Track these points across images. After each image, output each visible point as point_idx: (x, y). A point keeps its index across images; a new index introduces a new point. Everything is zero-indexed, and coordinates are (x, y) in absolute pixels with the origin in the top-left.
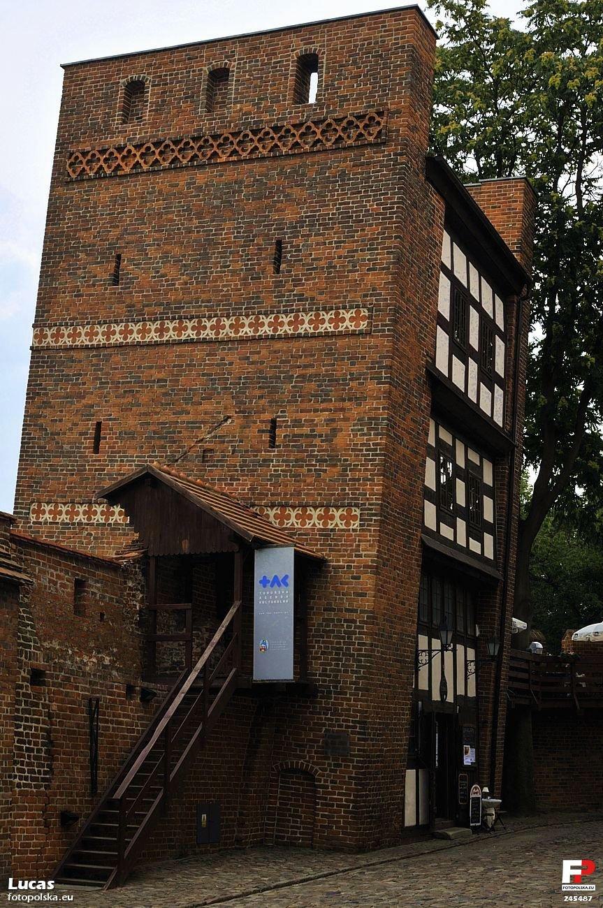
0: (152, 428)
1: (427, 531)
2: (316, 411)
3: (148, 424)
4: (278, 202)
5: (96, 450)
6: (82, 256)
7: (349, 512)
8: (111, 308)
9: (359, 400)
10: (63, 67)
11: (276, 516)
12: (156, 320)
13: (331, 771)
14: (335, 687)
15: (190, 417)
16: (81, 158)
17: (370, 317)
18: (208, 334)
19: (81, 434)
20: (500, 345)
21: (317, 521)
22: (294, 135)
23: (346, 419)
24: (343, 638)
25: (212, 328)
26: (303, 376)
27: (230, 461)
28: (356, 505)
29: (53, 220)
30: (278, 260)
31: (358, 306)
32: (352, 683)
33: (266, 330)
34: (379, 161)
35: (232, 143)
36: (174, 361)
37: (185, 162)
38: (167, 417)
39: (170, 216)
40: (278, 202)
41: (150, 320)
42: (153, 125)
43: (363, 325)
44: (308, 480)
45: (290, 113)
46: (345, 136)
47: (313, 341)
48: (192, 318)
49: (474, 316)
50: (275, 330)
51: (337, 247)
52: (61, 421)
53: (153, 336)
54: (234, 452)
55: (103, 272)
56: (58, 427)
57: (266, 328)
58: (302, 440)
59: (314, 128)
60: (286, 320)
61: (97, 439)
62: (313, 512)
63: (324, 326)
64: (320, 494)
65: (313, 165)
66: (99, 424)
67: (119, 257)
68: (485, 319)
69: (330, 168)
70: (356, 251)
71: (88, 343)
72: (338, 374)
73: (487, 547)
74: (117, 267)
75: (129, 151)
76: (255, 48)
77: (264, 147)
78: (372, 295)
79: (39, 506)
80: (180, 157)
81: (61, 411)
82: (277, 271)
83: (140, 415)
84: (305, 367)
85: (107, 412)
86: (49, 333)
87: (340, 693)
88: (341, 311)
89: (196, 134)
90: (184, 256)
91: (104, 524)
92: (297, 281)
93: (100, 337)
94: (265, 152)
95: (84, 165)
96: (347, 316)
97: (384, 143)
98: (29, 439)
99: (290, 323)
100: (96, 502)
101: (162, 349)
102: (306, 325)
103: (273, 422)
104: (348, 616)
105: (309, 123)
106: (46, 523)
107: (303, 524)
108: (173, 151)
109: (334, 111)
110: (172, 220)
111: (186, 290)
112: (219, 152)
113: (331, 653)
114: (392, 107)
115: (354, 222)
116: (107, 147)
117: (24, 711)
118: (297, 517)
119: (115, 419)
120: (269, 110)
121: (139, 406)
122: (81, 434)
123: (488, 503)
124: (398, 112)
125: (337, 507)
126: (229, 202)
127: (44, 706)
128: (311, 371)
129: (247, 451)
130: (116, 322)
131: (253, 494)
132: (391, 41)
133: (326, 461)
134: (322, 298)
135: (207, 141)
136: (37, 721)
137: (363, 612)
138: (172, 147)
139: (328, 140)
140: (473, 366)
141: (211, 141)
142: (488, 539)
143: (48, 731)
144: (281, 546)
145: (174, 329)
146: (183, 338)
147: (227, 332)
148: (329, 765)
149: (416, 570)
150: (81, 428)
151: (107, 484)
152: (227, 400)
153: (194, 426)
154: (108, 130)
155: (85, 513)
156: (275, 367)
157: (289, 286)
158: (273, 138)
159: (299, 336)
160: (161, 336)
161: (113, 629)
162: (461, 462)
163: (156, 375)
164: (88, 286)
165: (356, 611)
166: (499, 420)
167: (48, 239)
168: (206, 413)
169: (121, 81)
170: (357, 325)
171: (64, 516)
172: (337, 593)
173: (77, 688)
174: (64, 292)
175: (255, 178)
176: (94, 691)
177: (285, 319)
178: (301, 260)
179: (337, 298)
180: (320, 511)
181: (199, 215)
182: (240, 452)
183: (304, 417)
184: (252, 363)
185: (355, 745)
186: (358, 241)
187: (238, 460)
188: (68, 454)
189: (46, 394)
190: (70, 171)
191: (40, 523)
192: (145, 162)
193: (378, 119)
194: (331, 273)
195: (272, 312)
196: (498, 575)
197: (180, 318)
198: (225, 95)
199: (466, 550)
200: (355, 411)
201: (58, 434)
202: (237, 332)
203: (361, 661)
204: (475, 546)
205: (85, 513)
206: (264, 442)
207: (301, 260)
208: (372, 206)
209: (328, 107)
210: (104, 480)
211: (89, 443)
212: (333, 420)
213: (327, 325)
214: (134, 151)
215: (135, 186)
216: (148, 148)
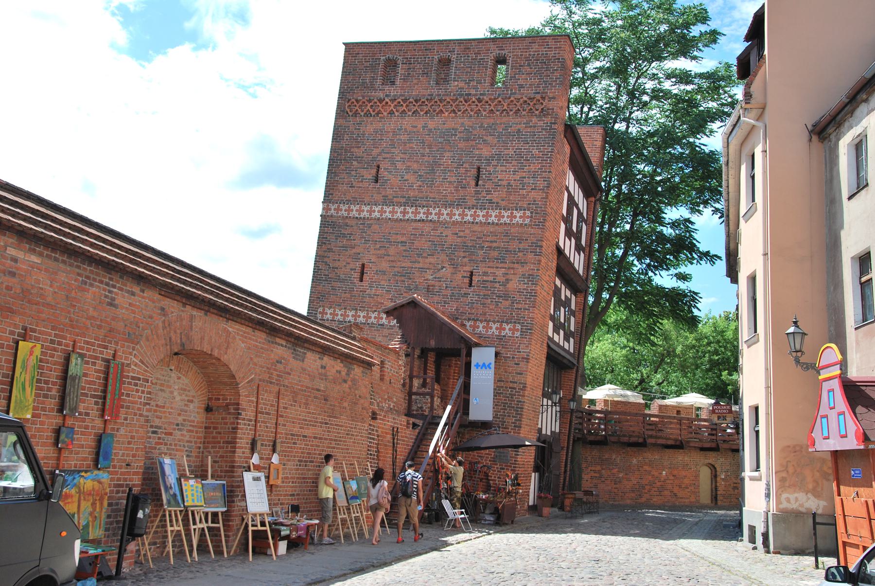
0: (396, 269)
1: (549, 338)
2: (497, 268)
3: (395, 267)
4: (479, 144)
5: (361, 280)
6: (355, 163)
7: (514, 326)
8: (372, 196)
9: (523, 263)
10: (344, 44)
11: (470, 326)
12: (401, 206)
13: (498, 471)
14: (503, 425)
15: (421, 265)
16: (355, 103)
17: (531, 217)
18: (433, 217)
19: (351, 270)
20: (584, 227)
21: (495, 331)
22: (490, 105)
23: (514, 274)
24: (508, 397)
25: (436, 214)
26: (490, 247)
27: (444, 292)
28: (519, 323)
29: (336, 139)
30: (478, 178)
31: (525, 210)
32: (514, 423)
33: (469, 218)
34: (541, 126)
35: (452, 105)
36: (410, 231)
37: (422, 113)
38: (407, 264)
39: (411, 145)
40: (479, 144)
41: (397, 206)
42: (402, 88)
43: (527, 221)
44: (491, 307)
45: (488, 91)
46: (521, 109)
47: (497, 227)
48: (424, 206)
49: (575, 211)
50: (474, 219)
51: (514, 174)
52: (339, 260)
53: (399, 215)
54: (446, 287)
55: (369, 174)
56: (337, 264)
57: (469, 217)
58: (488, 284)
59: (502, 103)
60: (481, 214)
61: (362, 273)
62: (493, 325)
63: (504, 219)
64: (498, 316)
65: (501, 124)
66: (363, 265)
67: (378, 167)
68: (580, 214)
69: (511, 127)
70: (525, 178)
71: (357, 216)
72: (511, 248)
73: (570, 346)
74: (378, 172)
75: (387, 103)
76: (468, 48)
77: (471, 111)
78: (533, 204)
79: (324, 310)
80: (419, 110)
81: (339, 255)
82: (477, 185)
83: (389, 261)
84: (491, 242)
85: (369, 257)
86: (333, 208)
87: (505, 428)
88: (515, 212)
89: (429, 98)
90: (419, 170)
91: (365, 324)
92: (489, 192)
93: (365, 213)
94: (472, 113)
95: (357, 108)
96: (518, 215)
97: (544, 115)
98: (318, 269)
99: (483, 216)
100: (360, 310)
101: (404, 224)
102: (493, 218)
103: (472, 273)
104: (511, 385)
105: (500, 99)
106: (328, 320)
107: (487, 331)
108: (414, 105)
109: (515, 93)
110: (413, 148)
111: (420, 191)
112: (444, 110)
113: (500, 405)
114: (551, 95)
115: (524, 160)
116: (372, 98)
117: (370, 434)
118: (484, 327)
119: (373, 262)
120: (476, 88)
121: (389, 255)
122: (351, 270)
123: (572, 319)
124: (554, 98)
125: (508, 324)
126: (449, 140)
127: (377, 431)
128: (494, 245)
129: (455, 288)
130: (376, 205)
131: (458, 312)
132: (551, 54)
133: (502, 297)
134: (503, 204)
135: (436, 102)
136: (373, 439)
137: (520, 383)
138: (414, 103)
139: (511, 111)
140: (573, 241)
141: (439, 103)
142: (572, 340)
143: (378, 444)
144: (485, 347)
145: (412, 213)
146: (418, 218)
147: (444, 217)
148: (497, 468)
149: (544, 361)
150: (352, 266)
151: (390, 305)
152: (443, 257)
153: (422, 270)
154: (372, 87)
155: (353, 316)
156: (473, 240)
157: (484, 194)
158: (477, 105)
159: (489, 223)
160: (404, 216)
161: (394, 388)
162: (563, 298)
163: (400, 239)
164: (358, 182)
165: (516, 383)
166: (581, 272)
167: (333, 150)
168: (430, 264)
169: (382, 58)
170: (524, 221)
171: (339, 317)
172: (506, 372)
173: (388, 421)
174: (343, 184)
175: (465, 127)
176: (395, 423)
177: (479, 212)
178: (491, 180)
179: (512, 204)
180: (498, 325)
181: (430, 147)
182: (450, 287)
183: (490, 271)
184: (460, 237)
185: (513, 457)
186: (525, 172)
187: (449, 293)
188: (343, 281)
189: (330, 244)
190: (348, 110)
191: (324, 320)
192: (397, 111)
193: (541, 101)
194: (508, 189)
195: (473, 208)
196: (575, 362)
197: (416, 206)
198: (447, 75)
199: (563, 348)
200: (520, 270)
201: (337, 268)
202: (451, 218)
203: (518, 411)
204: (566, 346)
205: (353, 316)
206: (464, 283)
207: (491, 180)
208: (535, 152)
209: (511, 90)
210: (366, 297)
211: (357, 275)
212: (507, 274)
213: (505, 219)
214: (389, 103)
215: (390, 124)
216: (399, 102)
